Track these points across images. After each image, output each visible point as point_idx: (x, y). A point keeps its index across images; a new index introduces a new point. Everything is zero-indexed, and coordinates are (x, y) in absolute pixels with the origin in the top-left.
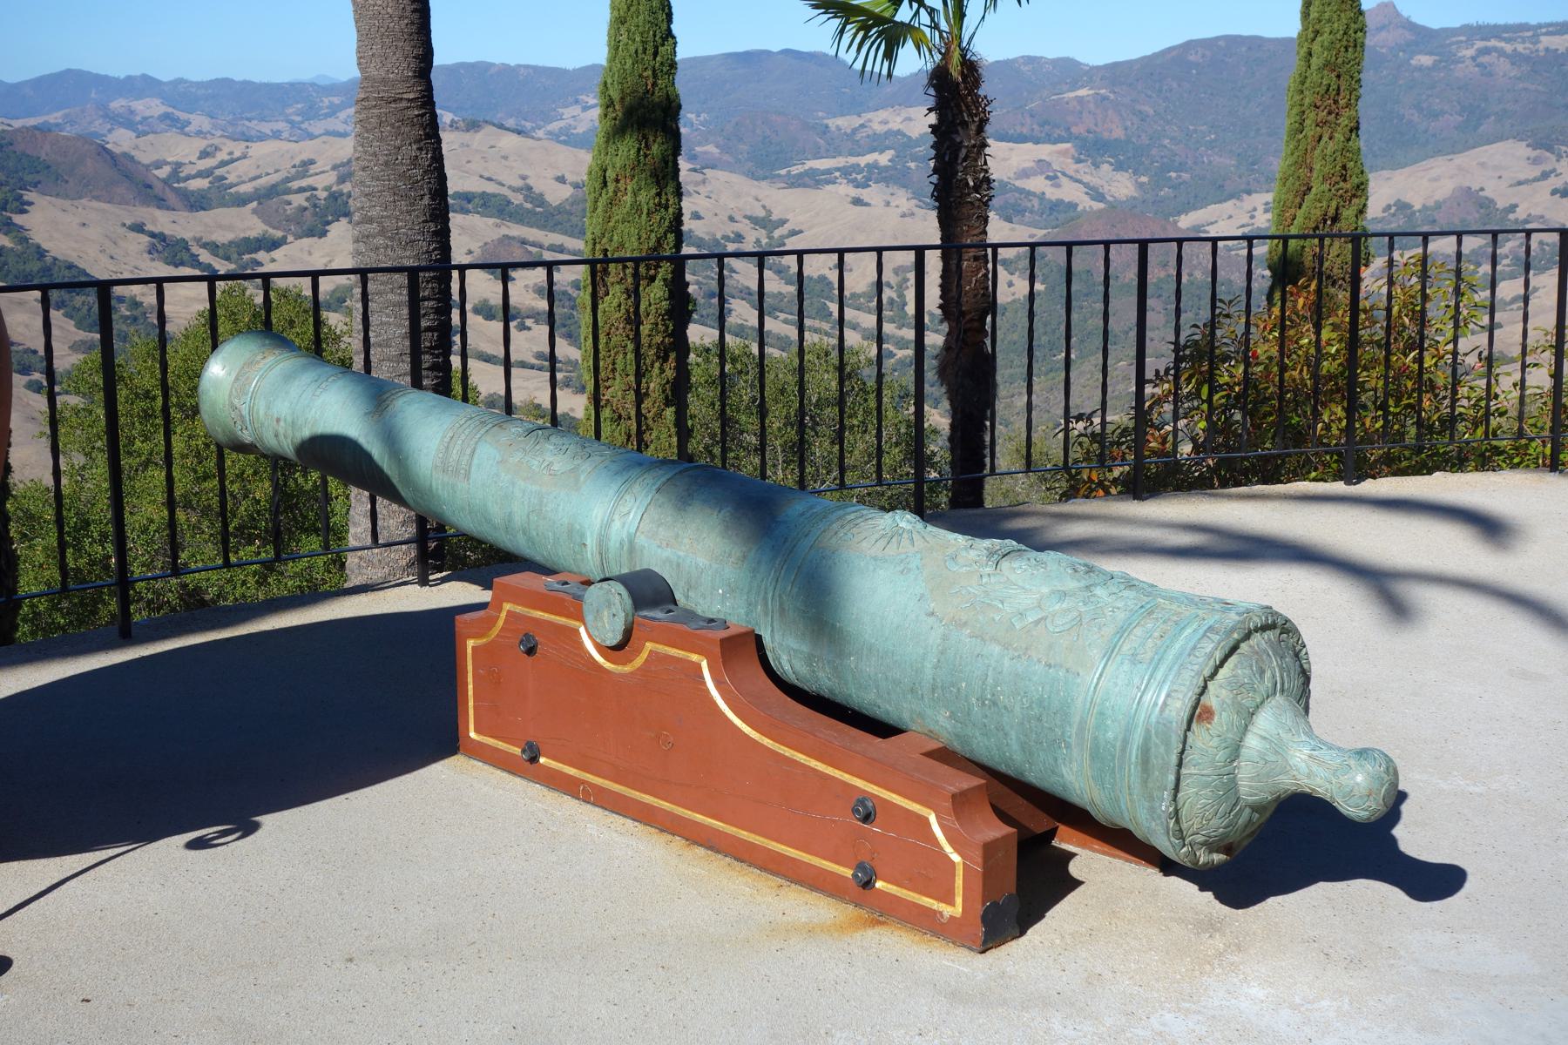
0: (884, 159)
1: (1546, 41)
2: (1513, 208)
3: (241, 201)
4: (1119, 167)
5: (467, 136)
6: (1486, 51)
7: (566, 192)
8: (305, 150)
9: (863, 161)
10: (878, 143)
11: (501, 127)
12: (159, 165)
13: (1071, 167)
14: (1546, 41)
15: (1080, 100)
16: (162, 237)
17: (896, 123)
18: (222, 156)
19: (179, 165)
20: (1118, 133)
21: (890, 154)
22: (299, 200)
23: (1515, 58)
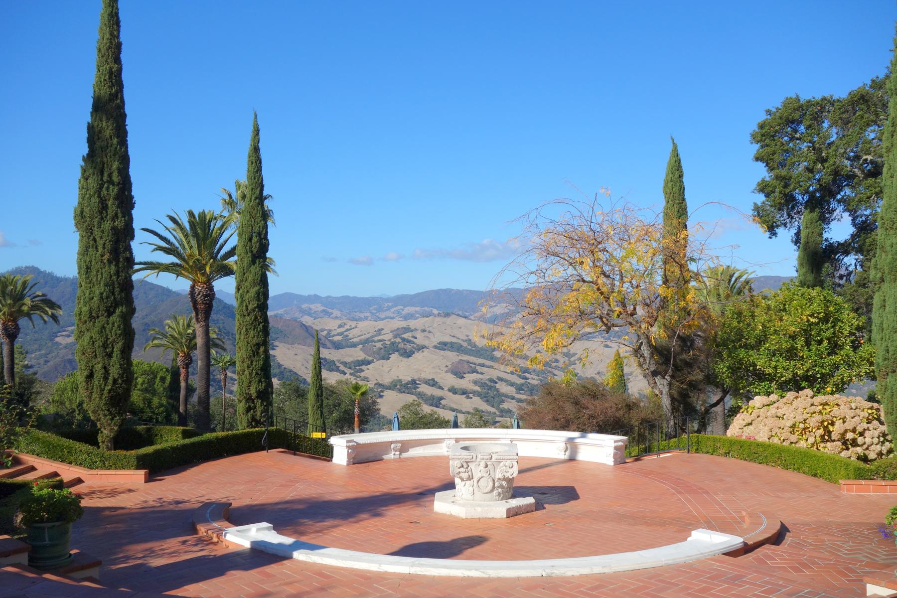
3: (354, 345)
8: (380, 324)
11: (458, 315)
22: (379, 345)
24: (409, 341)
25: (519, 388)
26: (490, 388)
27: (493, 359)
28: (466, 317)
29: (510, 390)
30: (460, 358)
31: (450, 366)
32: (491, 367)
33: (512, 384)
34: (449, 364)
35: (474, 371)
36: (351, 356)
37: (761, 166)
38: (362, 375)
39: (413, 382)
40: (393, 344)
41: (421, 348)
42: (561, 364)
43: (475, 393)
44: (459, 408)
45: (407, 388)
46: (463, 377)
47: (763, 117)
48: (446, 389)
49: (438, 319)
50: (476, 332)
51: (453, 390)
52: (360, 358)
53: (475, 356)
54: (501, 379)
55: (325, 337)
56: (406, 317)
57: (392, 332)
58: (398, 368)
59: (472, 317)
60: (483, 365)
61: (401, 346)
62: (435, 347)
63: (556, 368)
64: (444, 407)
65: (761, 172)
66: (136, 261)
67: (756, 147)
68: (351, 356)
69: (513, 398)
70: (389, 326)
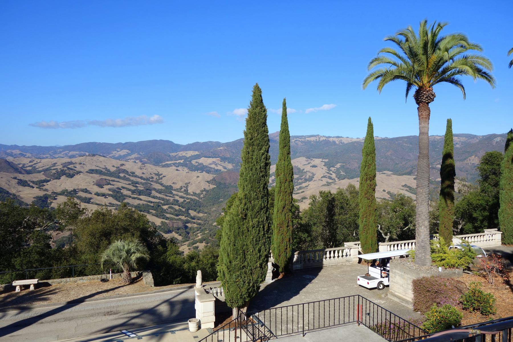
0: (182, 161)
1: (307, 139)
2: (304, 169)
3: (39, 172)
4: (229, 163)
5: (92, 158)
6: (297, 140)
7: (115, 169)
8: (54, 161)
9: (177, 162)
10: (180, 158)
11: (100, 155)
12: (19, 164)
13: (220, 163)
14: (307, 139)
15: (221, 149)
16: (21, 180)
17: (184, 154)
18: (35, 162)
19: (24, 164)
20: (229, 156)
21: (183, 160)
22: (54, 171)
23: (302, 142)
24: (72, 169)
25: (133, 192)
26: (118, 192)
27: (119, 177)
28: (104, 157)
29: (129, 193)
30: (101, 177)
31: (95, 182)
32: (119, 182)
33: (129, 190)
34: (95, 181)
35: (109, 184)
36: (37, 178)
38: (44, 188)
39: (75, 190)
40: (62, 171)
41: (79, 172)
42: (154, 179)
43: (109, 195)
44: (101, 203)
45: (71, 194)
46: (103, 187)
48: (93, 193)
49: (88, 158)
50: (111, 164)
51: (97, 194)
52: (43, 179)
53: (110, 176)
54: (124, 188)
55: (21, 168)
56: (73, 156)
57: (62, 164)
58: (67, 184)
60: (114, 181)
62: (87, 172)
63: (152, 181)
64: (92, 203)
66: (416, 132)
68: (37, 178)
69: (130, 197)
70: (60, 162)
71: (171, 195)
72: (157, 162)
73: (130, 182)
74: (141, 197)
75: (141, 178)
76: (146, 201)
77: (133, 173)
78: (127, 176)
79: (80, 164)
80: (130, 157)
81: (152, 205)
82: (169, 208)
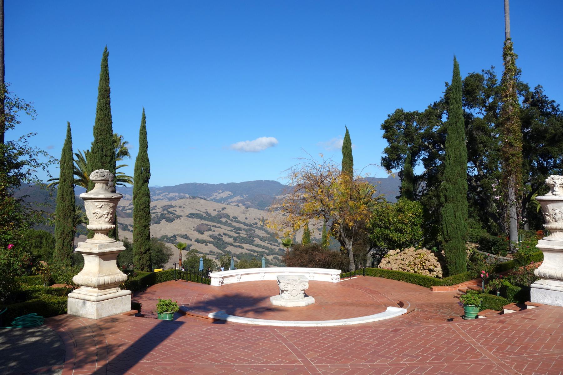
5: (192, 200)
7: (216, 213)
11: (201, 198)
19: (124, 207)
24: (172, 213)
26: (219, 239)
28: (205, 199)
29: (231, 240)
31: (196, 227)
32: (220, 227)
33: (230, 237)
37: (386, 140)
39: (175, 236)
41: (179, 217)
46: (203, 234)
47: (386, 118)
48: (193, 240)
49: (189, 200)
50: (212, 208)
51: (198, 241)
53: (211, 221)
54: (225, 234)
59: (208, 199)
60: (215, 226)
61: (167, 215)
62: (187, 216)
63: (256, 227)
65: (385, 144)
67: (383, 132)
69: (232, 245)
71: (277, 244)
72: (261, 206)
73: (232, 229)
74: (244, 245)
75: (244, 224)
76: (249, 250)
77: (235, 218)
78: (229, 221)
79: (180, 207)
80: (232, 200)
81: (255, 254)
82: (274, 258)
